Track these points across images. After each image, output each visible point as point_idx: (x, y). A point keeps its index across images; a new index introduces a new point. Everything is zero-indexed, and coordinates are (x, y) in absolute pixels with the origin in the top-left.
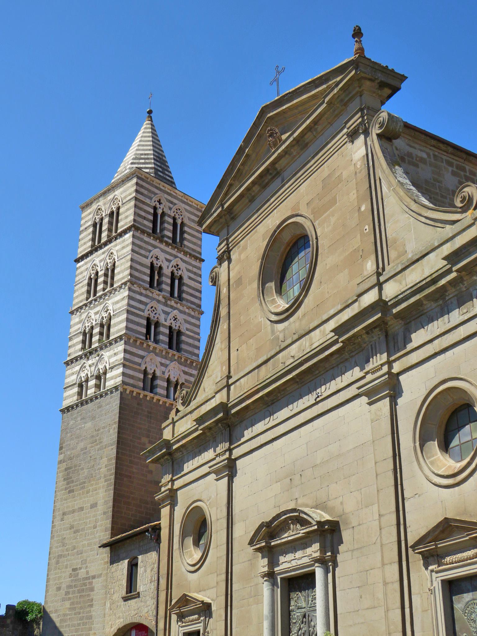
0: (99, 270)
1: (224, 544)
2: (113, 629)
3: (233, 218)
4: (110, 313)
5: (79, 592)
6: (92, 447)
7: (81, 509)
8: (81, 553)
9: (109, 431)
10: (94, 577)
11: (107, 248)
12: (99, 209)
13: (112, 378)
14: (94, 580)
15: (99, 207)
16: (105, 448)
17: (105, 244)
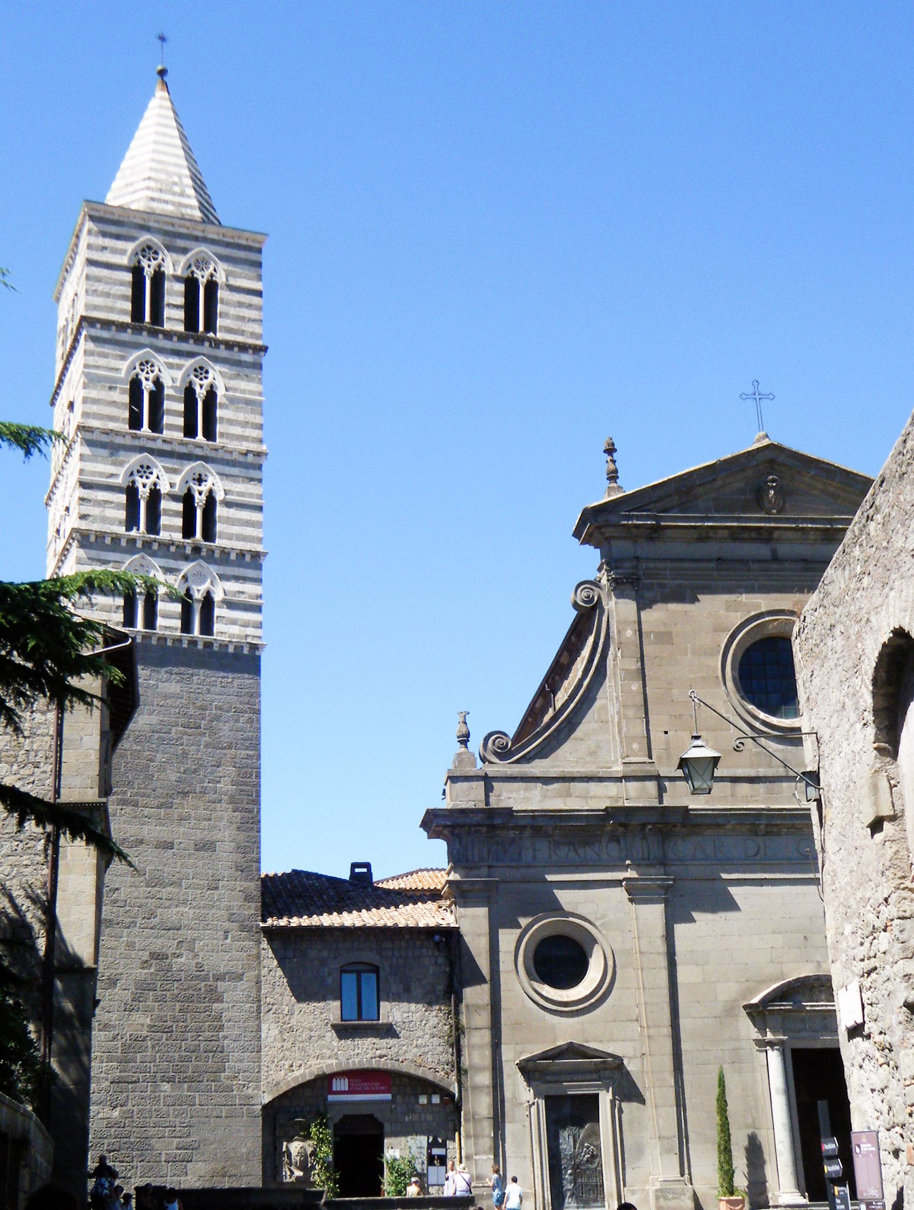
0: (166, 381)
1: (661, 988)
2: (297, 1073)
3: (651, 539)
4: (211, 492)
5: (175, 998)
6: (185, 733)
7: (170, 845)
8: (179, 929)
9: (237, 721)
10: (219, 978)
11: (184, 347)
12: (149, 248)
13: (233, 622)
14: (219, 983)
15: (150, 243)
16: (230, 748)
17: (182, 338)
